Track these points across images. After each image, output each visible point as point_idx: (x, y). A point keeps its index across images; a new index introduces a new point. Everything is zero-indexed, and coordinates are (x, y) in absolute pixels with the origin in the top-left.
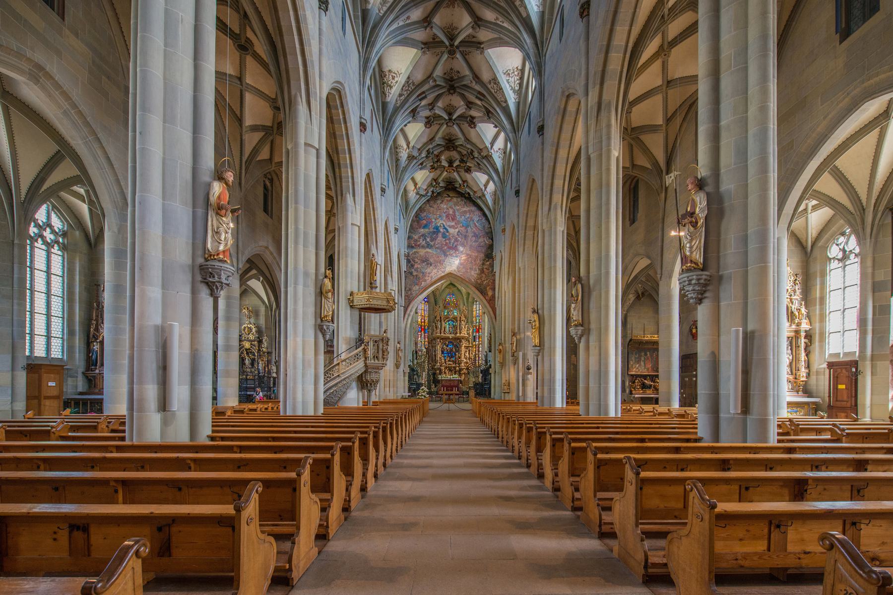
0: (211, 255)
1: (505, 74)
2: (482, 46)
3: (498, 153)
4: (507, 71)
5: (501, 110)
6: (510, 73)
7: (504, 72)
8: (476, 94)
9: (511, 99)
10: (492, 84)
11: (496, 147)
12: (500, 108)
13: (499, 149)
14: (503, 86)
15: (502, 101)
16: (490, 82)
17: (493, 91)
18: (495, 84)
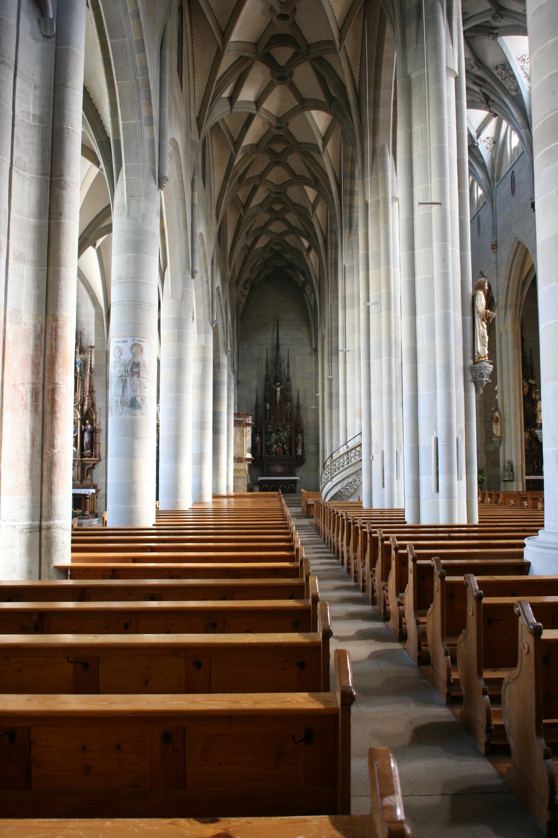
0: (479, 358)
1: (519, 59)
2: (496, 31)
3: (486, 142)
4: (522, 57)
5: (510, 100)
6: (526, 58)
7: (519, 57)
8: (473, 79)
9: (525, 88)
10: (500, 70)
11: (483, 136)
12: (508, 98)
13: (488, 138)
14: (516, 74)
15: (511, 90)
16: (497, 68)
17: (500, 77)
18: (504, 69)
